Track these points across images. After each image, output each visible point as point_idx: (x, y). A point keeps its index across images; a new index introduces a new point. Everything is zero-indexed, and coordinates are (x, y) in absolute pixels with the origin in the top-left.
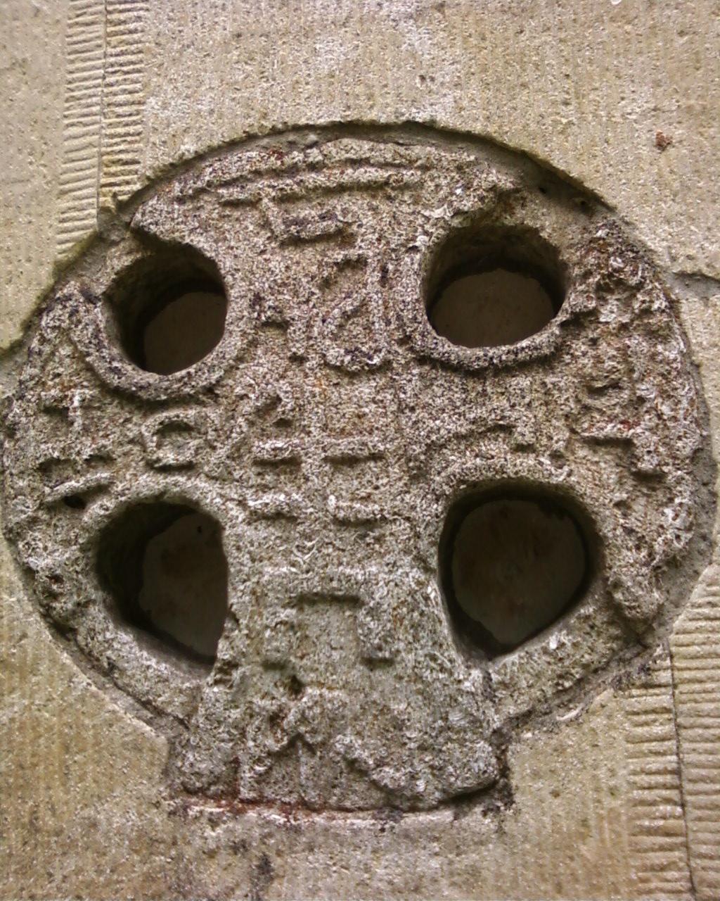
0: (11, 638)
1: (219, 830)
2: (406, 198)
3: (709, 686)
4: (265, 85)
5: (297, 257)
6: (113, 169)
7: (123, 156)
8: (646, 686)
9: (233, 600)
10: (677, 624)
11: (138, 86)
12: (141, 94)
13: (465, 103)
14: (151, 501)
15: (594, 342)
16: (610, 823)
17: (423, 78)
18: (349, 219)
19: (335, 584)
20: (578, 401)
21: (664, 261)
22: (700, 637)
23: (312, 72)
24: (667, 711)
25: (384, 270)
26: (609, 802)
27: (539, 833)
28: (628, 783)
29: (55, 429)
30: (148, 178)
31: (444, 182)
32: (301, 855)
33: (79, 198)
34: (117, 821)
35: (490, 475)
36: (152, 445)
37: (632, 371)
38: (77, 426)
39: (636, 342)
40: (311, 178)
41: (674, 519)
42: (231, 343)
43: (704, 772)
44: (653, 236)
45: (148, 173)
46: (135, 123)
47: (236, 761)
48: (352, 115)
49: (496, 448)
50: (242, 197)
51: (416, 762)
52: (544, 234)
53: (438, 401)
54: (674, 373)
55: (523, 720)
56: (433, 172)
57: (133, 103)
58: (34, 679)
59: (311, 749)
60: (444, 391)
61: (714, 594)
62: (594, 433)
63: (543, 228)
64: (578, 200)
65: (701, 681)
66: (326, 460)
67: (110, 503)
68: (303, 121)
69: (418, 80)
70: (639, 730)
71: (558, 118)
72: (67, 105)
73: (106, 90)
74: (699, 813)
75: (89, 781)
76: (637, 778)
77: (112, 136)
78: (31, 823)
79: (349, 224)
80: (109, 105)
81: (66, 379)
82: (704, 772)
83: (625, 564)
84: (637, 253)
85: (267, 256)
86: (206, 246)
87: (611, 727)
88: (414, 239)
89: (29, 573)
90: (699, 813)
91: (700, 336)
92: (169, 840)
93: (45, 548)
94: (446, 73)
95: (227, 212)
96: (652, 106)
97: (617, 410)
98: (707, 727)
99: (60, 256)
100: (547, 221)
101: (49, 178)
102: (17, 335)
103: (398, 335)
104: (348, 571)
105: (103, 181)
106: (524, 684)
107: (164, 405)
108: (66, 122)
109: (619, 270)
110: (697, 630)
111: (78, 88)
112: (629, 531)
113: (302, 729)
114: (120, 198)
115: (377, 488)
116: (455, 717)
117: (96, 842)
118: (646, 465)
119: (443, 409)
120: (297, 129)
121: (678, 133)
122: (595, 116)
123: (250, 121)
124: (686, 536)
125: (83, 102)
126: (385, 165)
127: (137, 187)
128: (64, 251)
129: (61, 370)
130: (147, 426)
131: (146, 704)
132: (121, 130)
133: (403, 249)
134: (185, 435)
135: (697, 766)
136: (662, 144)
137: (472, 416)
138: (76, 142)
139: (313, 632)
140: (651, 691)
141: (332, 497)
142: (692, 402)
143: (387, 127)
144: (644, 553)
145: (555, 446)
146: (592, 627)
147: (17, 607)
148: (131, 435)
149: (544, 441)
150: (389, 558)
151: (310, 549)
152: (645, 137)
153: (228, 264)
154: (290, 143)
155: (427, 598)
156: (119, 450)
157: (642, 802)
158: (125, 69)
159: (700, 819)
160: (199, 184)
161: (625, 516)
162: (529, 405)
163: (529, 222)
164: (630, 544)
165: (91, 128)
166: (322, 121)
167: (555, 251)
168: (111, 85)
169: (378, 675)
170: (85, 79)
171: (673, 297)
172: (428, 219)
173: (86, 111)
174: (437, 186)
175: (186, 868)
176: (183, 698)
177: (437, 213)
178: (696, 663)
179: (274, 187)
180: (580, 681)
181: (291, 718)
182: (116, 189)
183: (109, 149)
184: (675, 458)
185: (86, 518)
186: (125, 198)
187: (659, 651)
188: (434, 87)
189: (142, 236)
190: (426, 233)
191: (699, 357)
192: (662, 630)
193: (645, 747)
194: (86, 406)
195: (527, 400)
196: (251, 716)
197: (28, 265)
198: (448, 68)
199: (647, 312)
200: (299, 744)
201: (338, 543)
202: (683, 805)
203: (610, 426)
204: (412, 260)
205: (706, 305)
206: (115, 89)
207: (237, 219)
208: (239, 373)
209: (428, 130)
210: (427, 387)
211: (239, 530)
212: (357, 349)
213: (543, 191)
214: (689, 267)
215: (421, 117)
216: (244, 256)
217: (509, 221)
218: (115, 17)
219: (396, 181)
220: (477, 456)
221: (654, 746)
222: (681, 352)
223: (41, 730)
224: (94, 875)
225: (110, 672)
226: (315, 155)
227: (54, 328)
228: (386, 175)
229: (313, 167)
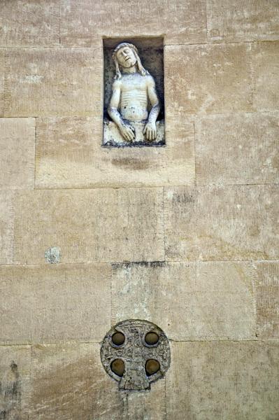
42: (125, 343)
44: (167, 335)
55: (153, 382)
60: (146, 349)
84: (165, 337)
100: (157, 332)
119: (146, 351)
209: (146, 321)
216: (127, 334)
225: (112, 376)
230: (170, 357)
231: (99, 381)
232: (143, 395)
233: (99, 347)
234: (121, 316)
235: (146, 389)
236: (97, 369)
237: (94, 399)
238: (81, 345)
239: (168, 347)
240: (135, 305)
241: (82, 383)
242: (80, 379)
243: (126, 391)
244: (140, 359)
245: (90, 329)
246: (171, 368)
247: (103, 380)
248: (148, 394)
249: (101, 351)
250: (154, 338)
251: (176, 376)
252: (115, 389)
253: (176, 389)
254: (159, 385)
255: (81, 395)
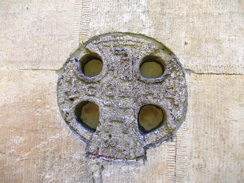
0: (58, 123)
1: (94, 160)
2: (138, 48)
3: (182, 142)
4: (113, 23)
5: (117, 57)
6: (83, 36)
7: (85, 34)
8: (171, 141)
9: (100, 120)
10: (178, 131)
11: (88, 19)
12: (89, 21)
13: (151, 32)
14: (86, 101)
15: (169, 80)
16: (163, 164)
17: (143, 26)
18: (127, 51)
19: (119, 119)
20: (165, 90)
21: (184, 67)
22: (181, 134)
23: (122, 21)
24: (175, 146)
25: (133, 62)
26: (163, 160)
27: (151, 164)
28: (167, 157)
29: (69, 85)
30: (89, 39)
31: (145, 46)
32: (109, 166)
33: (76, 41)
34: (76, 157)
35: (149, 102)
36: (87, 90)
37: (175, 86)
38: (73, 85)
39: (177, 81)
40: (121, 43)
41: (180, 113)
42: (104, 72)
43: (180, 157)
44: (182, 61)
45: (90, 38)
46: (87, 27)
47: (98, 148)
48: (130, 32)
49: (150, 97)
50: (107, 45)
51: (130, 151)
52: (162, 58)
53: (141, 88)
54: (183, 87)
56: (143, 44)
57: (87, 23)
58: (62, 131)
59: (112, 147)
61: (185, 126)
62: (168, 96)
63: (162, 57)
64: (169, 52)
65: (181, 141)
66: (119, 96)
67: (79, 100)
68: (120, 31)
69: (142, 26)
70: (169, 148)
71: (167, 36)
72: (74, 21)
73: (82, 19)
74: (178, 163)
75: (71, 150)
76: (168, 157)
77: (83, 29)
78: (60, 157)
79: (127, 52)
80: (82, 22)
81: (71, 76)
82: (180, 157)
83: (170, 119)
85: (111, 57)
86: (100, 54)
87: (165, 148)
88: (139, 56)
89: (62, 112)
90: (178, 163)
91: (188, 81)
92: (85, 162)
93: (66, 107)
94: (148, 25)
95: (104, 47)
96: (185, 36)
97: (172, 93)
98: (181, 149)
99: (71, 52)
100: (163, 55)
101: (70, 36)
102: (62, 67)
103: (134, 74)
104: (121, 117)
105: (81, 38)
106: (150, 139)
107: (90, 83)
108: (73, 24)
109: (175, 67)
110: (181, 132)
111: (76, 18)
112: (172, 114)
113: (111, 143)
114: (84, 42)
115: (128, 103)
116: (138, 144)
117: (72, 161)
118: (176, 103)
120: (118, 32)
121: (189, 42)
122: (174, 37)
123: (110, 30)
124: (181, 116)
125: (77, 21)
126: (134, 42)
127: (87, 40)
128: (72, 51)
129: (70, 74)
130: (86, 87)
131: (82, 137)
132: (85, 28)
133: (137, 58)
134: (93, 89)
135: (178, 156)
136: (186, 43)
137: (146, 91)
138: (75, 29)
139: (114, 127)
140: (172, 142)
141: (120, 103)
142: (185, 93)
143: (136, 34)
144: (174, 118)
145: (161, 98)
146: (163, 130)
147: (60, 118)
148: (83, 88)
149: (159, 97)
150: (129, 115)
151: (115, 112)
152: (183, 42)
153: (104, 58)
154: (117, 35)
155: (135, 123)
156: (81, 91)
157: (169, 161)
158: (86, 15)
159: (178, 164)
160: (99, 41)
161: (171, 111)
162: (157, 90)
163: (160, 56)
164: (172, 117)
165: (78, 27)
166: (123, 32)
167: (164, 61)
168: (83, 18)
169: (125, 135)
170: (78, 16)
171: (184, 73)
172: (142, 53)
173: (78, 23)
174: (144, 47)
175: (88, 167)
176: (89, 136)
177: (143, 52)
178: (180, 138)
179: (113, 43)
180: (160, 139)
181: (109, 141)
182: (83, 40)
183: (82, 32)
184: (181, 102)
185: (74, 103)
186: (85, 42)
187: (174, 135)
188: (145, 28)
189: (87, 50)
190: (141, 56)
191: (187, 84)
192: (175, 132)
193: (170, 151)
194: (75, 82)
195: (157, 89)
196: (102, 141)
197: (65, 53)
198: (148, 24)
199: (179, 76)
200: (110, 146)
201: (120, 112)
202: (175, 162)
203: (170, 95)
204: (138, 60)
205: (190, 75)
206: (83, 19)
207: (106, 49)
208: (104, 79)
209: (143, 35)
210: (139, 85)
211: (102, 108)
212: (127, 76)
213: (163, 50)
214: (188, 68)
215: (142, 33)
217: (156, 55)
218: (84, 4)
219: (136, 45)
220: (147, 99)
221: (172, 151)
222: (184, 83)
223: (63, 140)
224: (71, 167)
226: (121, 38)
227: (70, 66)
228: (135, 43)
229: (121, 40)
230: (186, 102)
231: (52, 138)
232: (131, 168)
233: (55, 77)
234: (100, 25)
235: (137, 158)
236: (48, 116)
237: (42, 169)
238: (26, 73)
239: (183, 83)
240: (125, 8)
241: (22, 139)
242: (19, 131)
243: (100, 160)
244: (129, 102)
245: (44, 46)
246: (189, 122)
247: (58, 135)
248: (142, 168)
249: (59, 84)
250: (157, 64)
251: (197, 139)
252: (79, 154)
253: (196, 162)
254: (162, 153)
255: (18, 159)
